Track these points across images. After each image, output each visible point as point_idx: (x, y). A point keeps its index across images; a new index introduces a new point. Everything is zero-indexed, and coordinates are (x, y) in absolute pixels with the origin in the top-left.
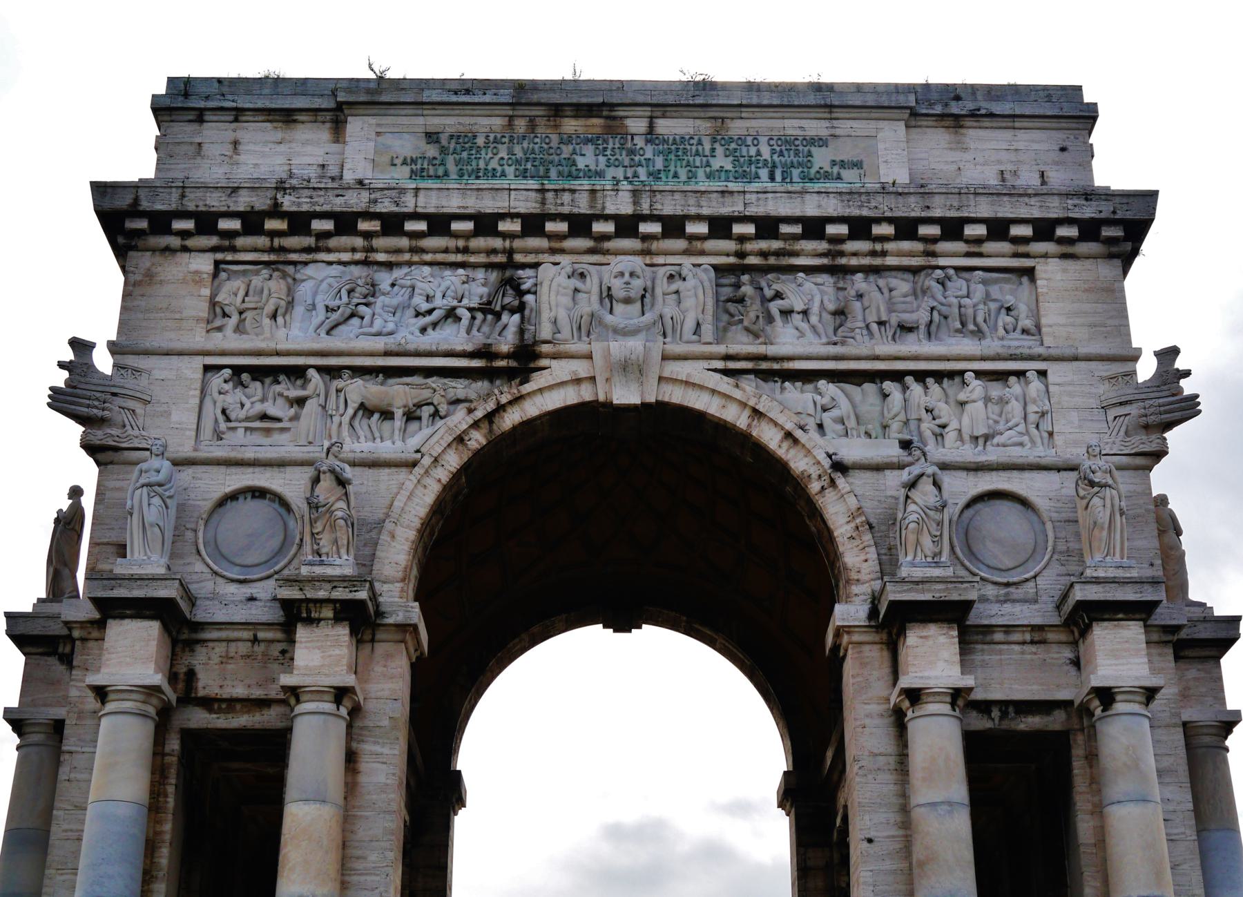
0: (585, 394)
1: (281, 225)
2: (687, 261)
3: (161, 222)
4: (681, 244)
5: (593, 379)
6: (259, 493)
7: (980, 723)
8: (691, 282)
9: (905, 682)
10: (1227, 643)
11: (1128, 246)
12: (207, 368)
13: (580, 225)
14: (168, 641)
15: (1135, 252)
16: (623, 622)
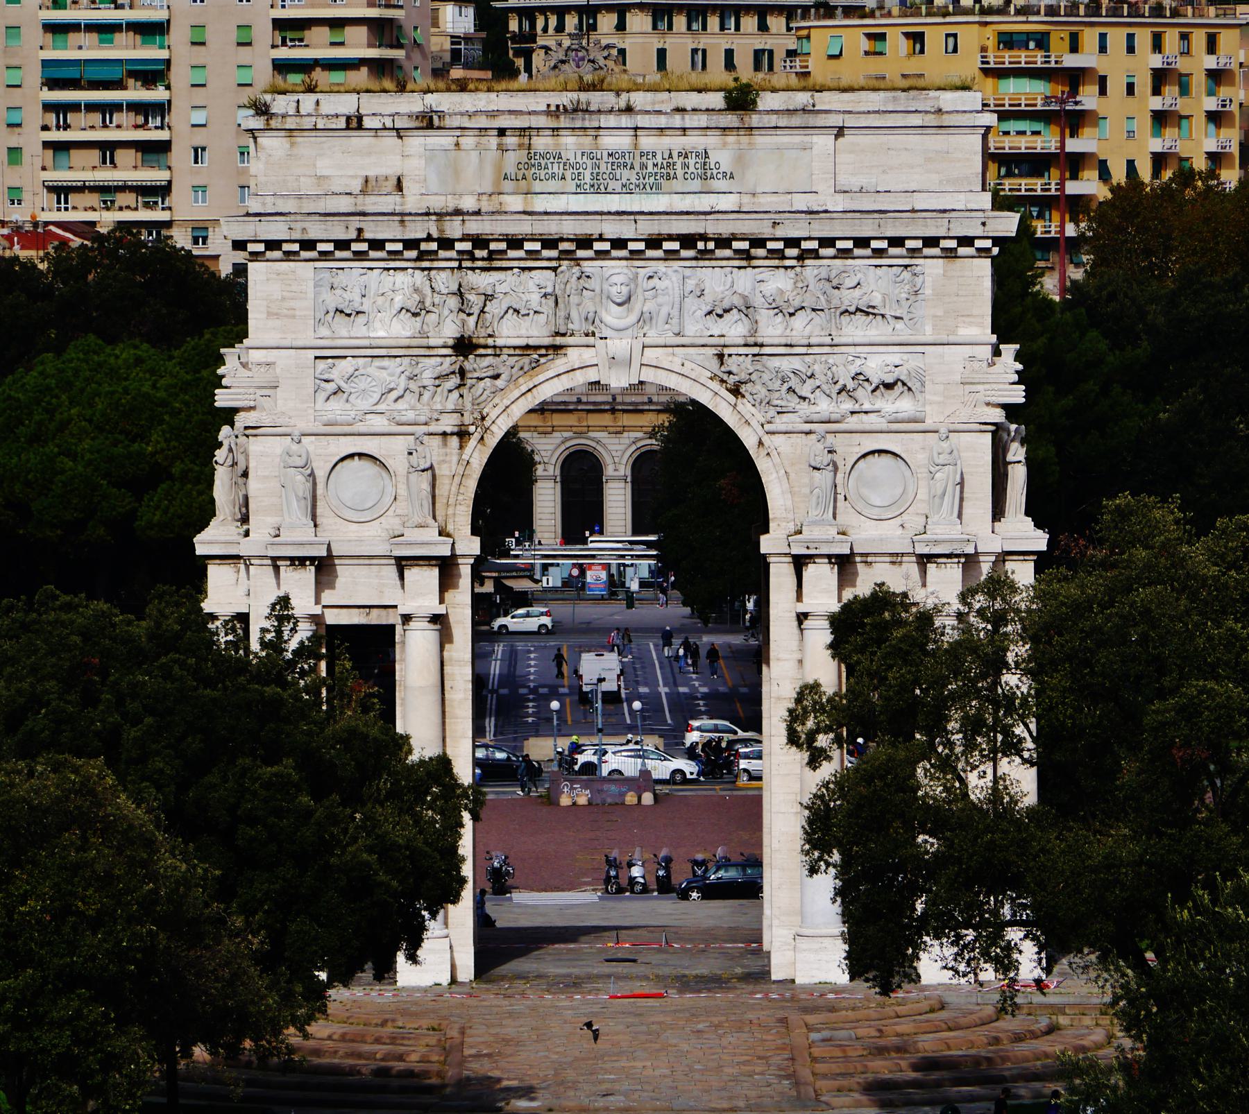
1: (364, 247)
2: (661, 267)
6: (361, 455)
12: (316, 358)
13: (585, 242)
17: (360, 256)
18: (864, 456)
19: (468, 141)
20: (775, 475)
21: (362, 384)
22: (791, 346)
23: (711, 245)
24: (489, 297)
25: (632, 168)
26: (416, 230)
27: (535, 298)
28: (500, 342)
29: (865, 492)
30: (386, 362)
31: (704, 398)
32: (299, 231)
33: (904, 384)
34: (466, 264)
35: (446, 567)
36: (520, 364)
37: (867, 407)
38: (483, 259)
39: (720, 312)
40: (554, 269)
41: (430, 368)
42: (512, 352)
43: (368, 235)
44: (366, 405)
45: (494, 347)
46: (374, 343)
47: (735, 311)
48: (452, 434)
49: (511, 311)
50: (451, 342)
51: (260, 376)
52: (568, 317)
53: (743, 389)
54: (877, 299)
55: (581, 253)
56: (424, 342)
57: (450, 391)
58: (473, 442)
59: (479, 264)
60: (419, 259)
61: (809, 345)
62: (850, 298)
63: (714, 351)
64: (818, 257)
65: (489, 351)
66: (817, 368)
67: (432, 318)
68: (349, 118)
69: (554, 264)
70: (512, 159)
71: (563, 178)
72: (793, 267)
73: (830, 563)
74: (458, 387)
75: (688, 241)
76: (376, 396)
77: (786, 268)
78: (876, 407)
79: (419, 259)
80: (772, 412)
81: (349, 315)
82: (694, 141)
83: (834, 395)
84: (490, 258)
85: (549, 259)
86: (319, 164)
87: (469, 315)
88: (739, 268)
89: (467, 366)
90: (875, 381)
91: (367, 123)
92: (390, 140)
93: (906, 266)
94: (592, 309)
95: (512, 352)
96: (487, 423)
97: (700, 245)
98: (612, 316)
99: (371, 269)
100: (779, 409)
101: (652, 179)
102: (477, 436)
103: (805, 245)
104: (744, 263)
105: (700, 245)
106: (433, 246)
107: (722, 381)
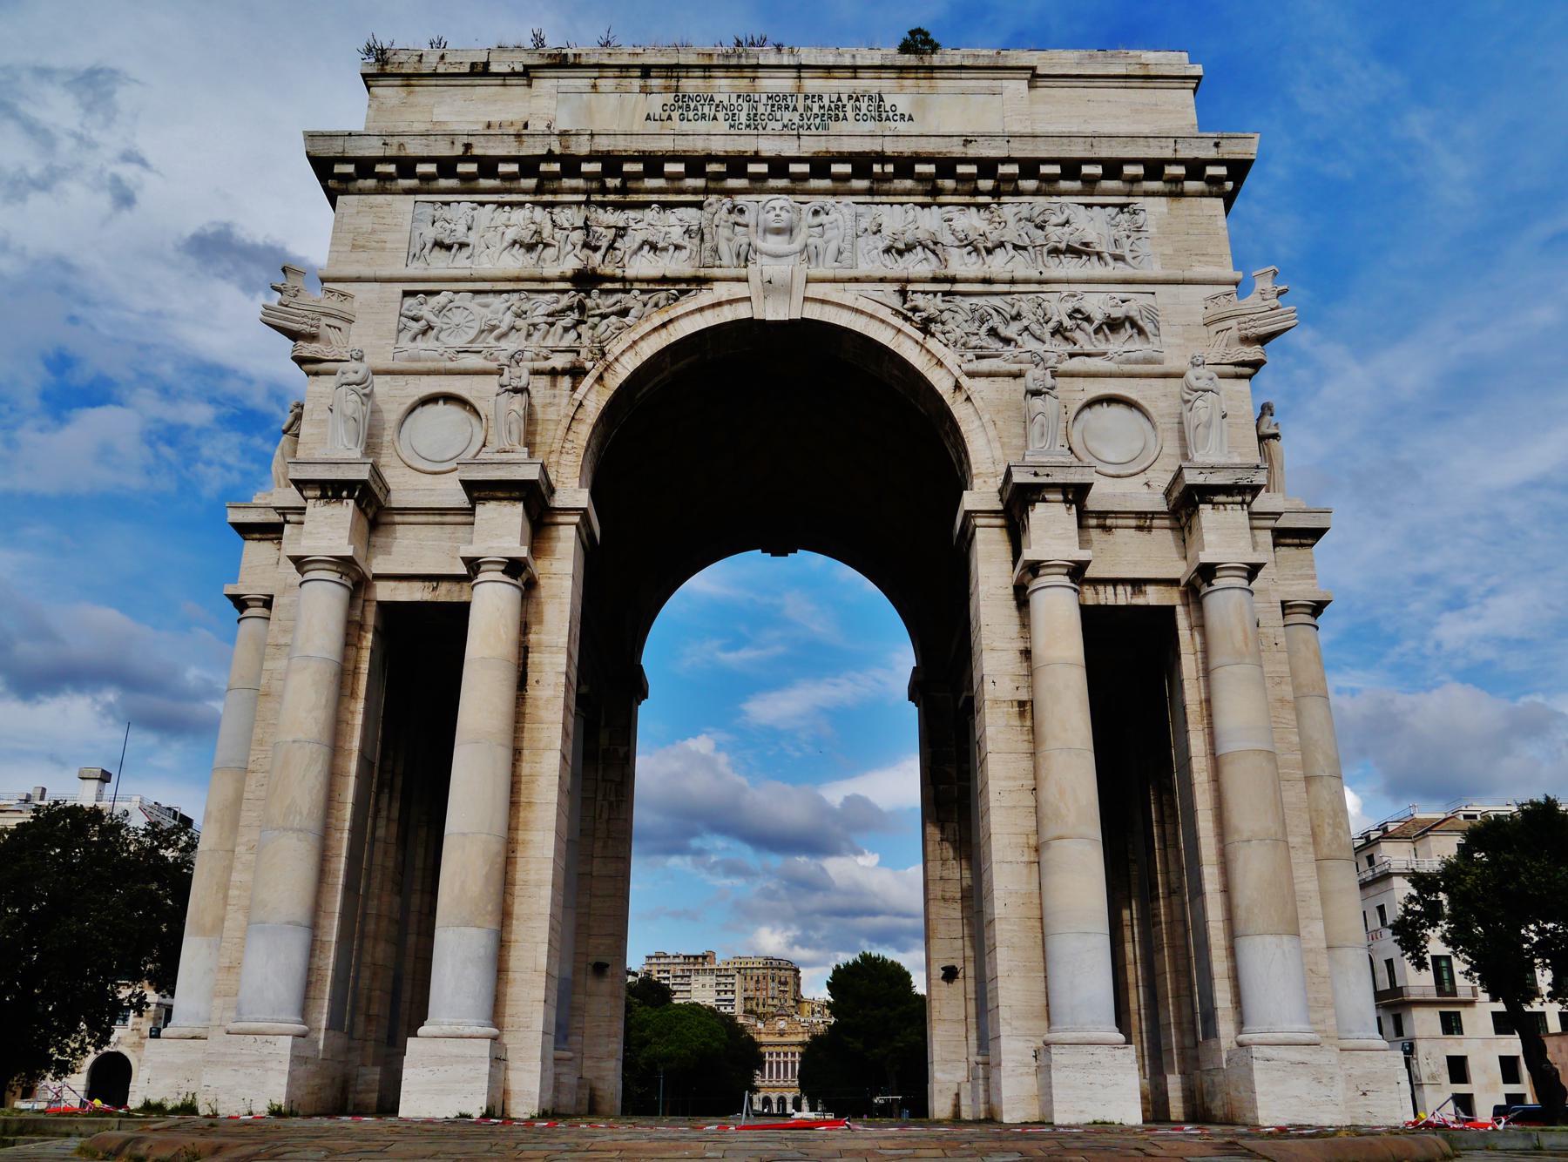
0: (742, 312)
1: (472, 168)
2: (830, 200)
3: (365, 166)
4: (826, 183)
5: (749, 299)
6: (449, 398)
7: (1091, 597)
8: (833, 216)
9: (1028, 554)
10: (1317, 533)
11: (1229, 185)
12: (406, 294)
13: (737, 164)
14: (364, 523)
15: (1236, 190)
16: (780, 548)
17: (468, 185)
18: (1090, 404)
19: (606, 84)
20: (977, 423)
21: (457, 317)
22: (986, 281)
23: (890, 168)
24: (621, 232)
25: (795, 109)
26: (536, 148)
27: (677, 235)
28: (630, 273)
29: (1092, 445)
30: (490, 299)
31: (883, 336)
32: (395, 148)
33: (1134, 324)
34: (599, 198)
35: (536, 501)
36: (655, 299)
37: (1088, 348)
38: (616, 191)
39: (901, 246)
40: (699, 205)
41: (544, 304)
42: (645, 286)
43: (476, 151)
44: (460, 341)
45: (623, 280)
46: (476, 274)
47: (919, 249)
48: (564, 372)
49: (646, 248)
50: (569, 273)
51: (333, 304)
52: (716, 250)
53: (933, 327)
54: (1090, 237)
55: (732, 183)
56: (536, 272)
57: (566, 330)
58: (588, 381)
59: (612, 197)
60: (538, 190)
61: (1013, 282)
62: (1057, 236)
63: (896, 287)
64: (1018, 192)
65: (618, 286)
66: (1025, 306)
67: (550, 252)
68: (473, 65)
69: (700, 198)
70: (656, 103)
71: (715, 118)
72: (986, 206)
73: (1066, 501)
74: (574, 327)
75: (862, 163)
76: (473, 333)
77: (979, 206)
78: (1102, 347)
79: (538, 190)
80: (970, 355)
81: (449, 248)
82: (866, 84)
83: (1047, 336)
84: (623, 190)
85: (695, 191)
86: (436, 111)
87: (596, 249)
88: (923, 206)
89: (589, 303)
90: (1098, 318)
91: (494, 68)
92: (517, 91)
93: (1122, 207)
94: (745, 240)
95: (645, 286)
96: (610, 358)
97: (877, 168)
98: (774, 243)
99: (482, 204)
100: (979, 352)
101: (818, 121)
102: (594, 373)
103: (1003, 169)
104: (928, 199)
105: (877, 168)
106: (556, 167)
107: (906, 318)
